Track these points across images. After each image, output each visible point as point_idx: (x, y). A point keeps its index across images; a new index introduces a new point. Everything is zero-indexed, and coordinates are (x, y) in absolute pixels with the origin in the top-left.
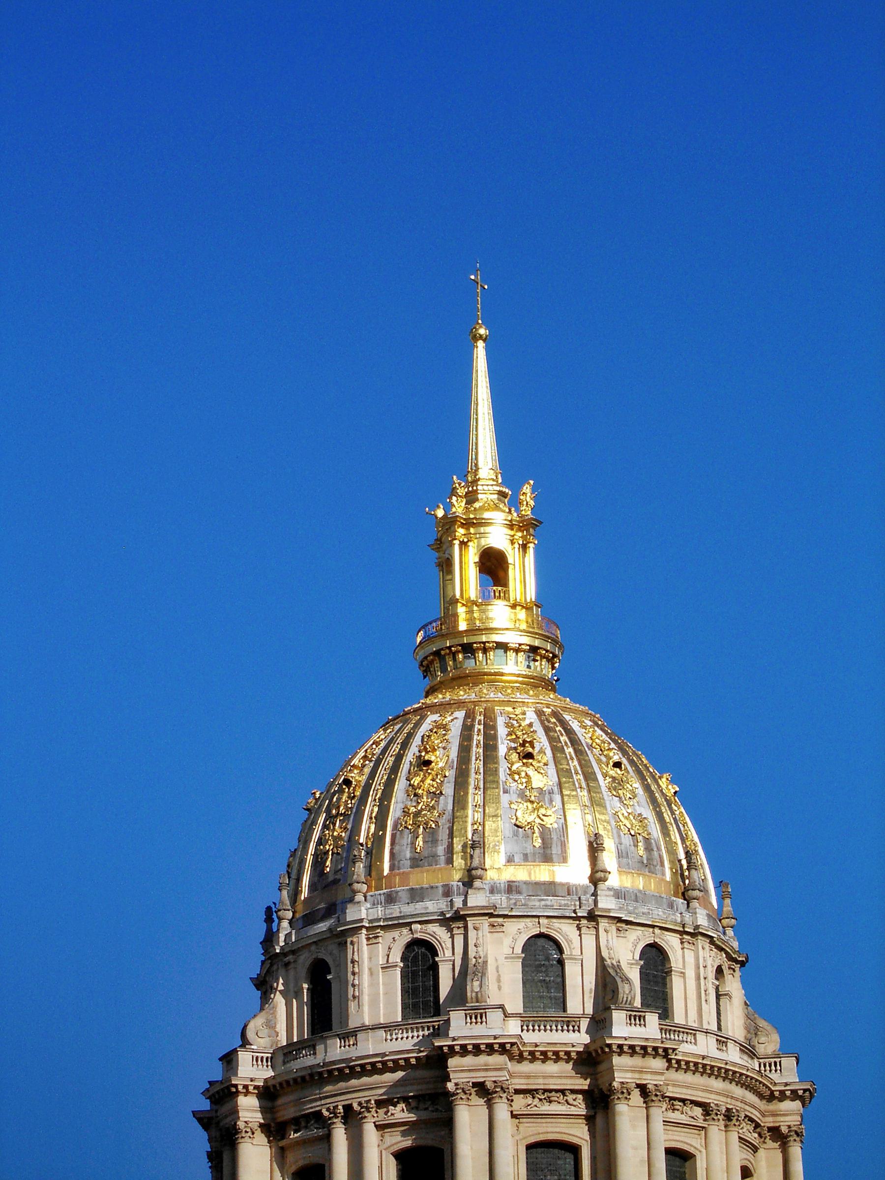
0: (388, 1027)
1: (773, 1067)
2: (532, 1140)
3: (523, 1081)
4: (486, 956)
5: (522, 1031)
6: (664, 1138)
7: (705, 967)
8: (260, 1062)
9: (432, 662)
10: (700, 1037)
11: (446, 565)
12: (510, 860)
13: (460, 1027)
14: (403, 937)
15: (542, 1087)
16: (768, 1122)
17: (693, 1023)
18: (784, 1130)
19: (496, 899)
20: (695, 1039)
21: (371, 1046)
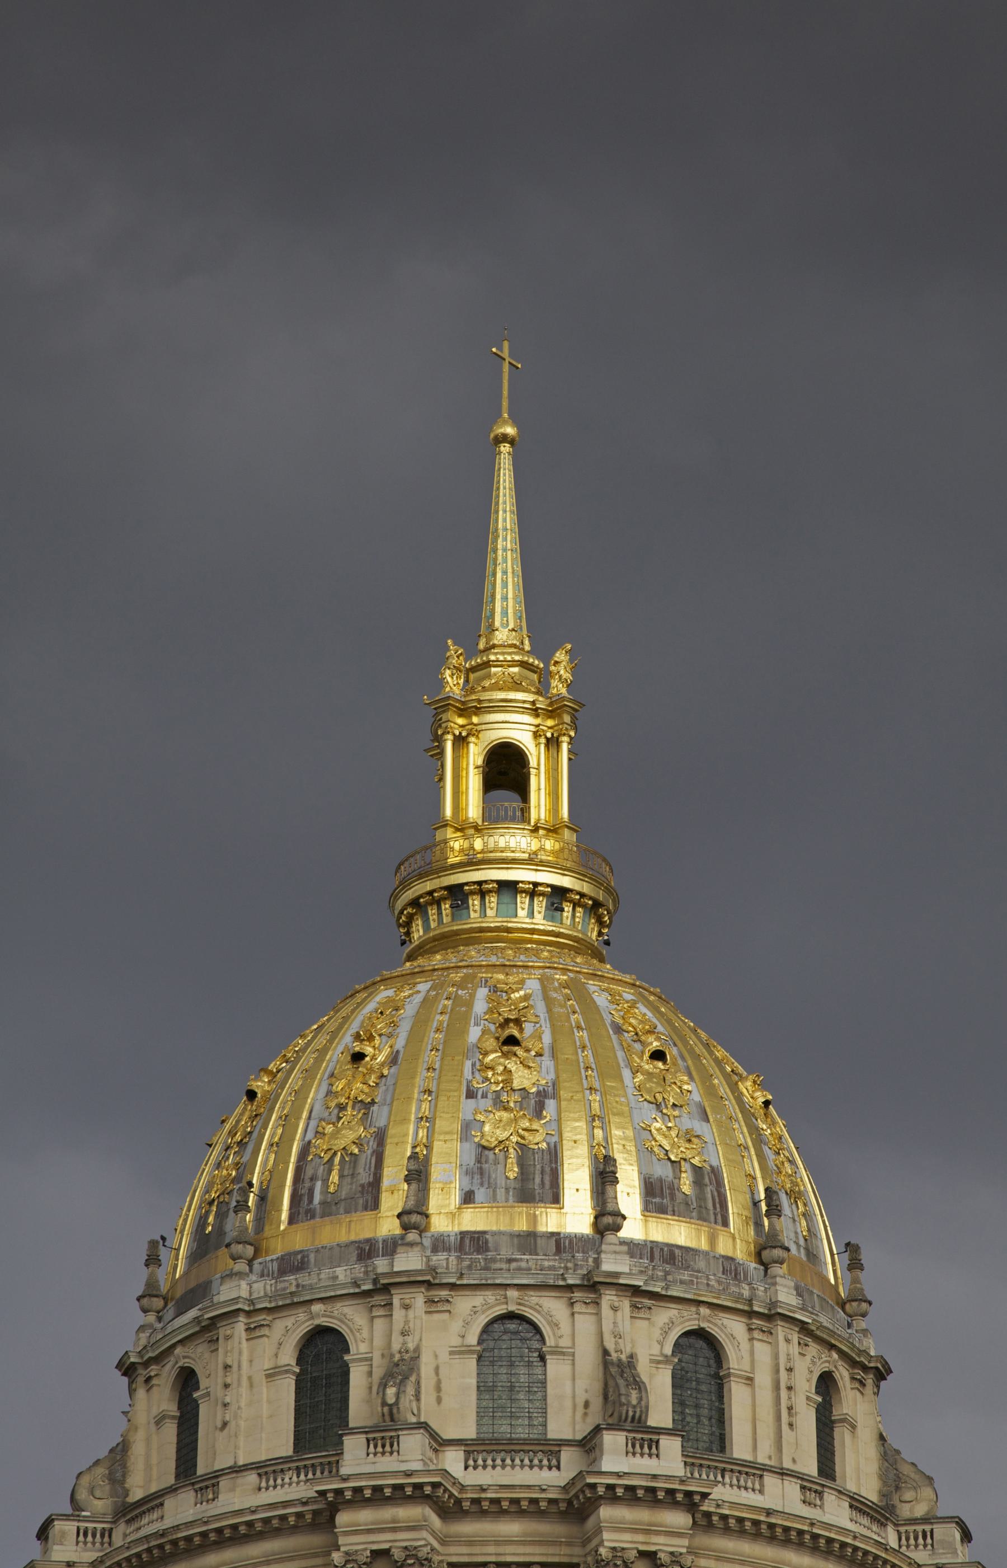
0: (268, 1470)
1: (921, 1541)
3: (464, 1550)
4: (417, 1349)
5: (466, 1468)
7: (790, 1370)
8: (90, 1538)
9: (411, 918)
10: (769, 1480)
12: (468, 1198)
13: (356, 1459)
15: (493, 1559)
17: (762, 1459)
19: (439, 1259)
20: (762, 1485)
21: (240, 1498)
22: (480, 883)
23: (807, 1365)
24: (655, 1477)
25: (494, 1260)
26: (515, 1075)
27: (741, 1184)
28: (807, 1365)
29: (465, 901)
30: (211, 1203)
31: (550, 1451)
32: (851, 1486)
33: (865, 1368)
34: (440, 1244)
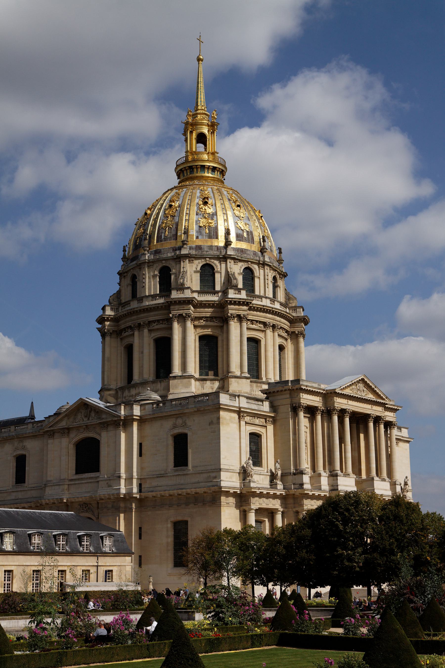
0: (154, 297)
2: (201, 334)
6: (247, 334)
7: (267, 275)
9: (180, 173)
10: (263, 299)
11: (186, 140)
13: (175, 295)
14: (160, 266)
16: (292, 330)
17: (262, 294)
18: (297, 332)
21: (147, 303)
22: (196, 166)
23: (271, 274)
24: (240, 299)
25: (203, 251)
26: (207, 210)
27: (257, 234)
28: (271, 274)
29: (193, 170)
30: (138, 238)
31: (216, 293)
32: (279, 300)
33: (282, 275)
34: (191, 248)
